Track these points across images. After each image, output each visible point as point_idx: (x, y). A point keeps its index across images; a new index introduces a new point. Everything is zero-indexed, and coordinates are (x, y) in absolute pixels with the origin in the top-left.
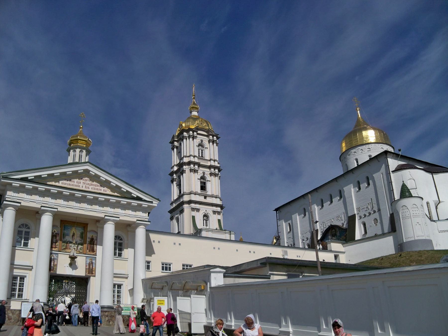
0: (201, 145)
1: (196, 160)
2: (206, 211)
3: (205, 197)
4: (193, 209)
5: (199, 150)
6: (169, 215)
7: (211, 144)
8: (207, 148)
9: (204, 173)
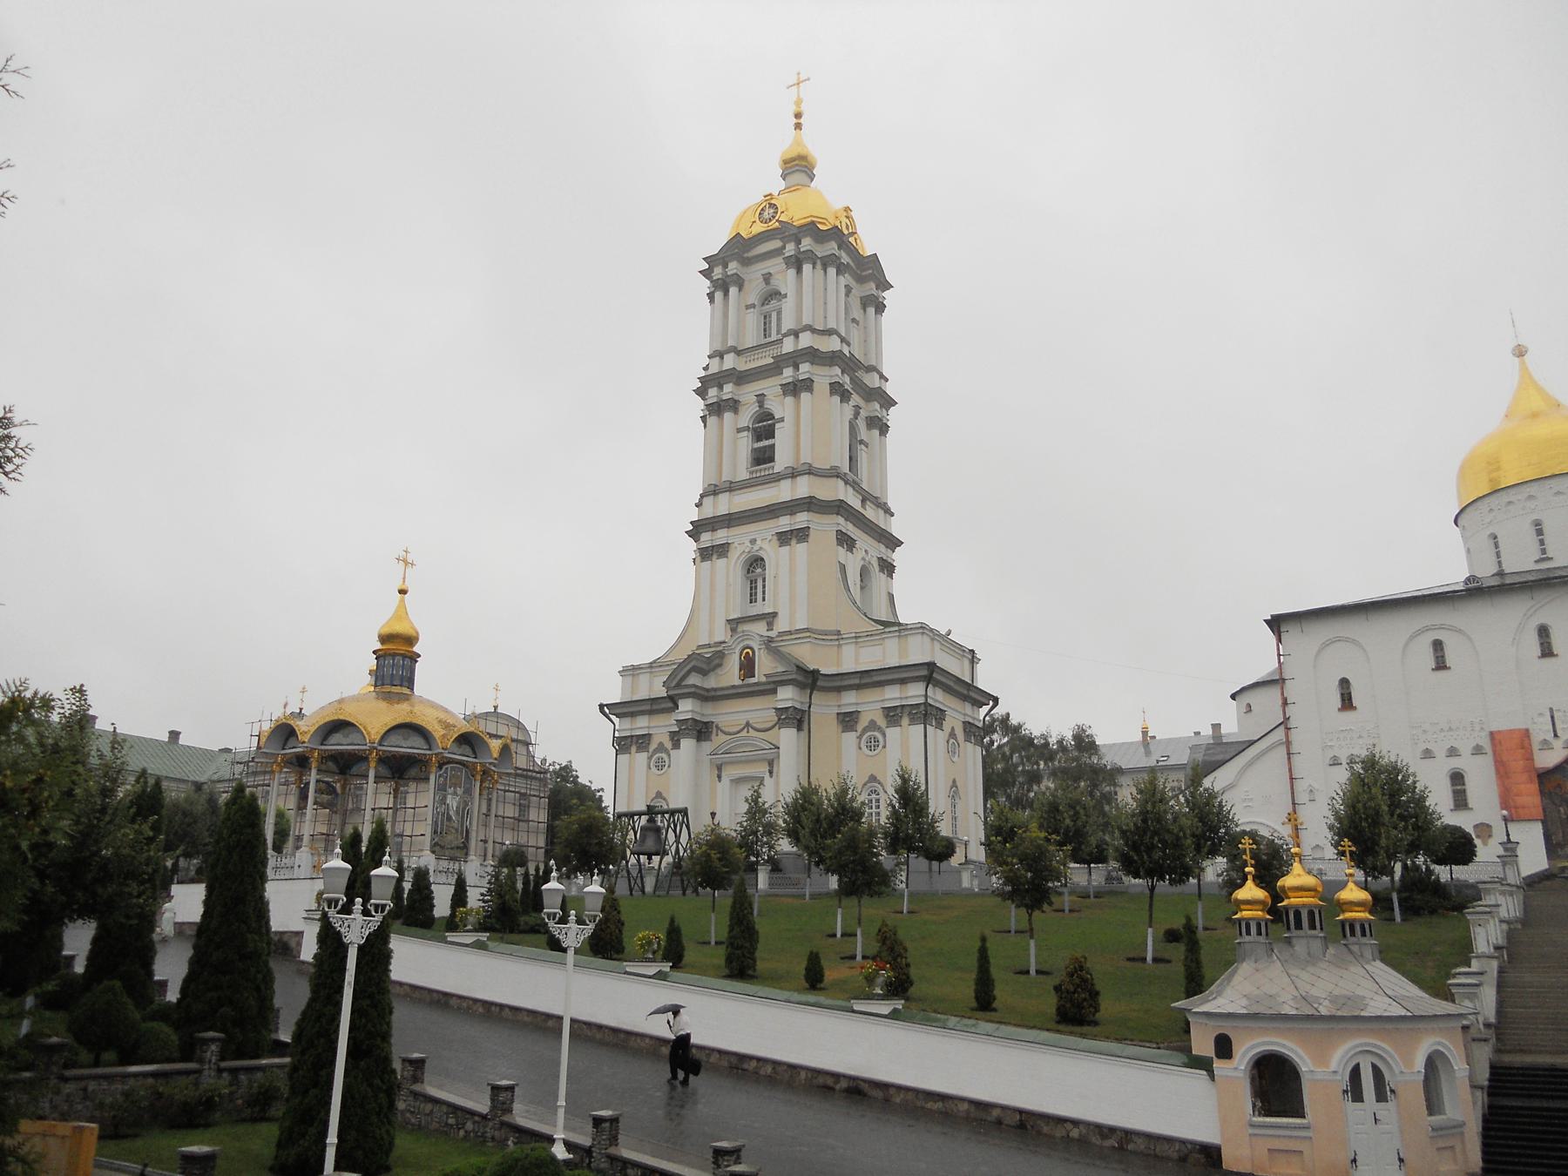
3: (863, 501)
7: (871, 310)
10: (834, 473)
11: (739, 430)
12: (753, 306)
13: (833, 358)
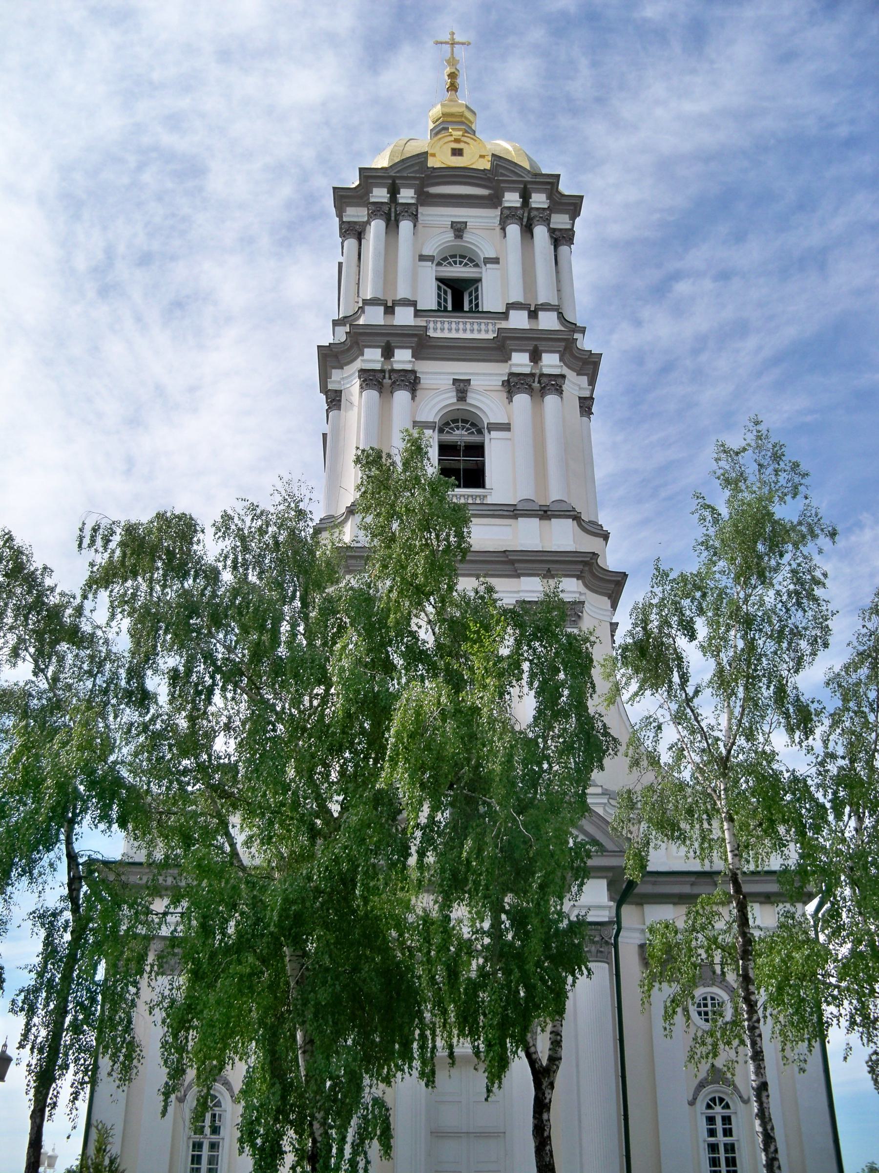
7: (514, 230)
8: (496, 261)
9: (462, 387)
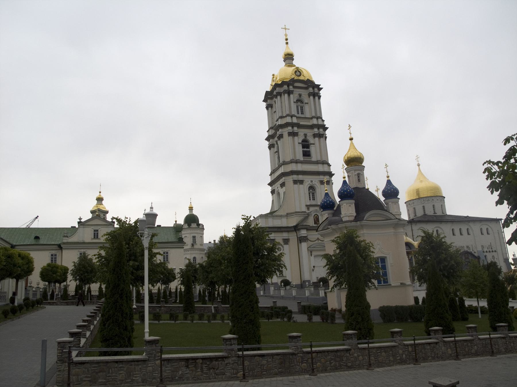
0: (299, 100)
1: (295, 120)
2: (312, 181)
4: (295, 182)
5: (297, 107)
6: (269, 188)
7: (312, 97)
8: (307, 103)
9: (305, 135)
10: (291, 162)
11: (275, 153)
12: (275, 112)
13: (287, 125)
